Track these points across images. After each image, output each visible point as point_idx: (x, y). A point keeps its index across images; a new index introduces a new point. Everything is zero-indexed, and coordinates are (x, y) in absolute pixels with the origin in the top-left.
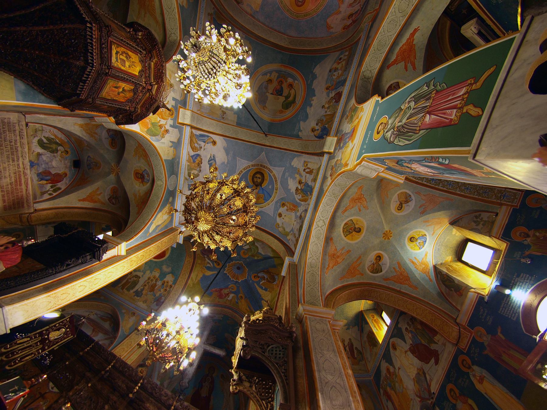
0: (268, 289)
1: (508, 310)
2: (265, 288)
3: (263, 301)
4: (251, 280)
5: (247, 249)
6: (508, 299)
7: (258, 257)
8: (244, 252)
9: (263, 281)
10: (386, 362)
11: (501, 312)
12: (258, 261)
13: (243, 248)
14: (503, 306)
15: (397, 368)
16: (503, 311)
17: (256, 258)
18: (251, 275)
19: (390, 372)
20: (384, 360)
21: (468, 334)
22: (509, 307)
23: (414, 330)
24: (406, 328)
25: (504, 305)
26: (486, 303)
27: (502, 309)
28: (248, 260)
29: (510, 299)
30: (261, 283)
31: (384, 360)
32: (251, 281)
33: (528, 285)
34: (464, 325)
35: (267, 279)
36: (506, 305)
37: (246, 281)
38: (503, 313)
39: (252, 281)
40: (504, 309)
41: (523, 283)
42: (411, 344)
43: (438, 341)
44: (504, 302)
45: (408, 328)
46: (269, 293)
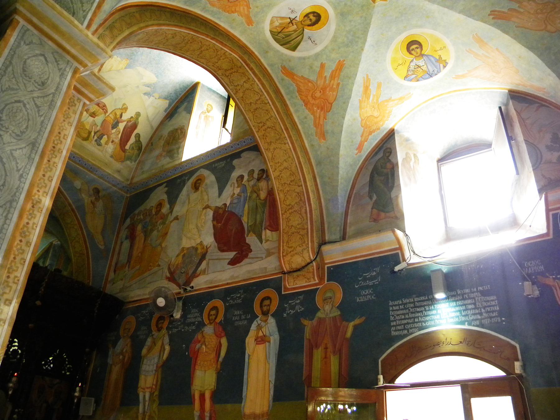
1: (404, 314)
6: (425, 303)
10: (167, 193)
11: (392, 306)
14: (406, 304)
15: (174, 214)
16: (397, 308)
19: (160, 210)
20: (166, 189)
21: (315, 280)
22: (412, 313)
23: (249, 190)
24: (242, 177)
25: (410, 303)
26: (394, 272)
27: (399, 305)
29: (429, 305)
31: (166, 189)
33: (476, 320)
34: (326, 262)
36: (412, 305)
38: (393, 311)
40: (401, 307)
41: (476, 308)
42: (225, 205)
43: (267, 241)
44: (416, 299)
45: (246, 178)
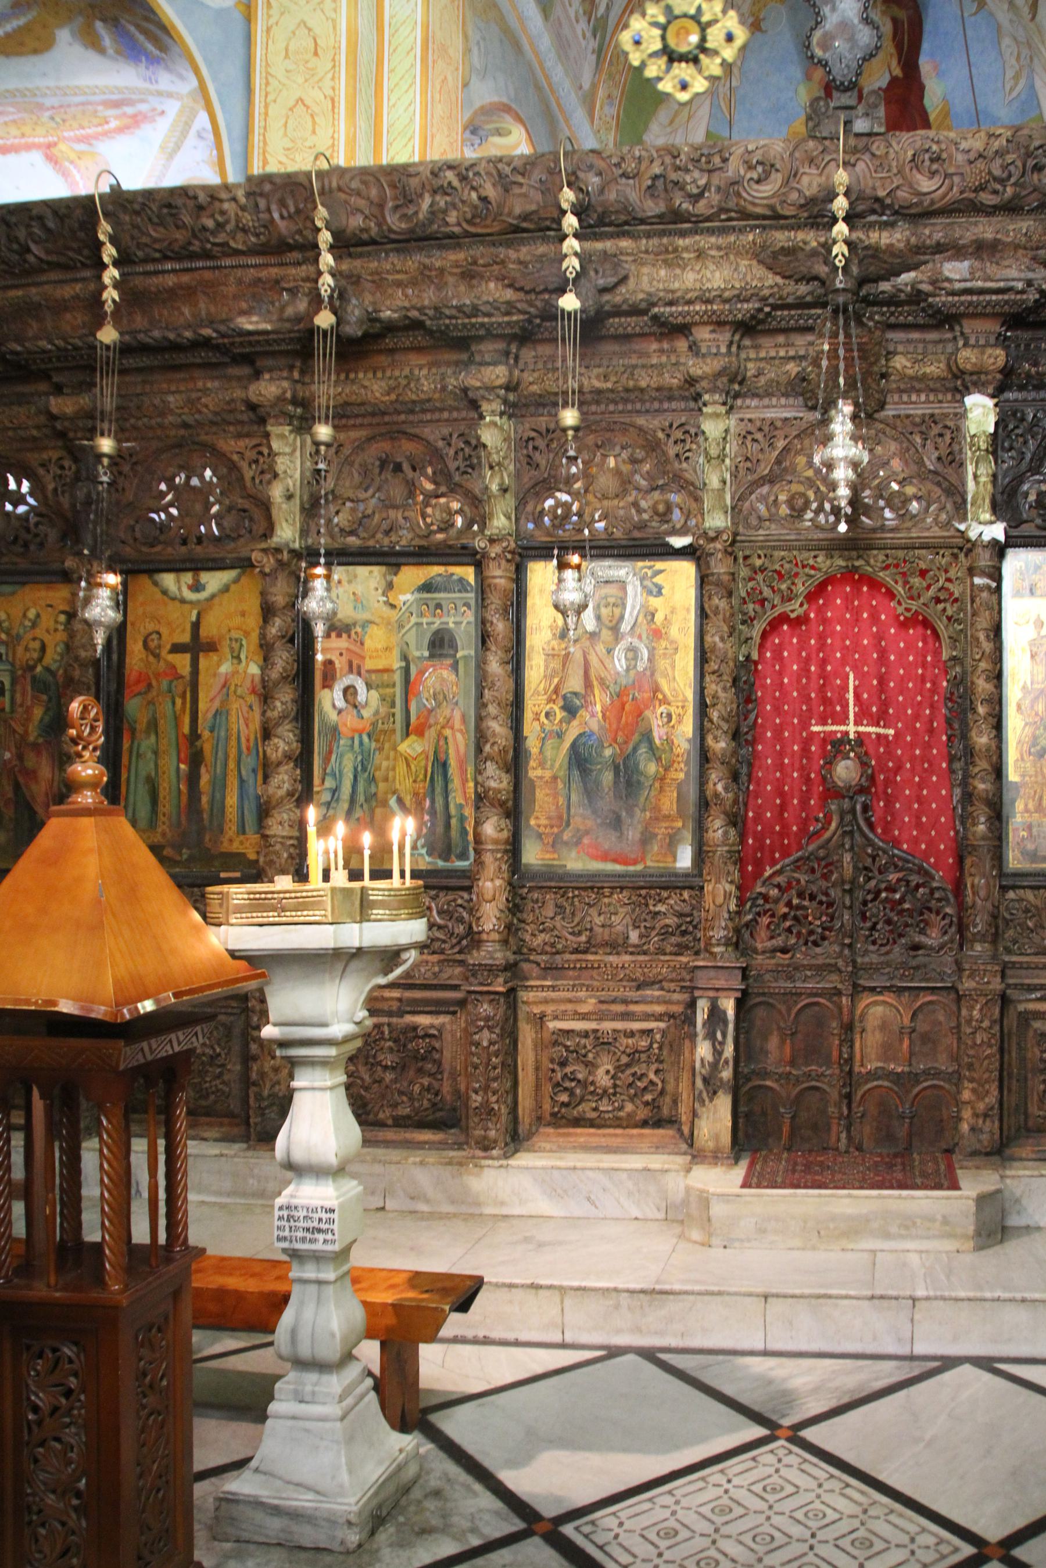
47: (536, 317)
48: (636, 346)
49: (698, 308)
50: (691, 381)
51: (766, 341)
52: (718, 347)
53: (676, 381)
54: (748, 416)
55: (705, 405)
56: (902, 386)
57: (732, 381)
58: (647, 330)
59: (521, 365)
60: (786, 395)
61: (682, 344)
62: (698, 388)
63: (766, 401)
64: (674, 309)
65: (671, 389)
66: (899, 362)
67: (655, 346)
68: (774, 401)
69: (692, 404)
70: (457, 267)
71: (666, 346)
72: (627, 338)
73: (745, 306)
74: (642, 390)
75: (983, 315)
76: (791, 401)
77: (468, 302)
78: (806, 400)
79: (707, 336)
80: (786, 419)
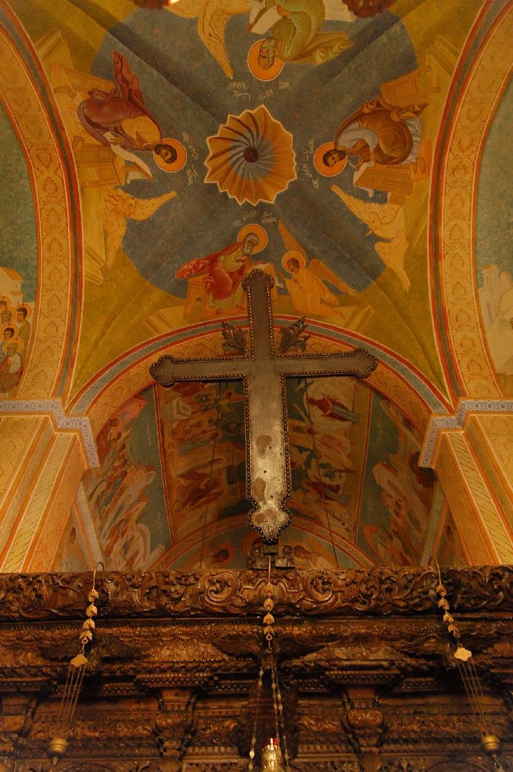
0: (389, 195)
2: (376, 192)
3: (379, 247)
4: (314, 178)
5: (273, 28)
7: (327, 48)
8: (262, 56)
9: (364, 166)
12: (331, 70)
13: (254, 30)
17: (319, 59)
18: (311, 159)
28: (285, 85)
30: (357, 176)
32: (315, 183)
35: (378, 150)
37: (297, 189)
39: (322, 178)
46: (396, 207)
47: (54, 680)
48: (121, 706)
49: (168, 676)
50: (157, 731)
51: (213, 705)
52: (179, 706)
53: (145, 732)
54: (196, 761)
55: (165, 750)
56: (310, 739)
57: (186, 732)
58: (131, 693)
59: (37, 716)
60: (225, 745)
61: (154, 706)
62: (162, 737)
63: (210, 749)
64: (152, 676)
65: (141, 738)
66: (306, 721)
67: (134, 707)
68: (216, 749)
69: (155, 751)
70: (9, 641)
71: (143, 706)
72: (114, 700)
73: (201, 675)
74: (120, 739)
75: (364, 686)
76: (229, 749)
77: (9, 666)
78: (240, 748)
79: (173, 698)
80: (224, 764)
